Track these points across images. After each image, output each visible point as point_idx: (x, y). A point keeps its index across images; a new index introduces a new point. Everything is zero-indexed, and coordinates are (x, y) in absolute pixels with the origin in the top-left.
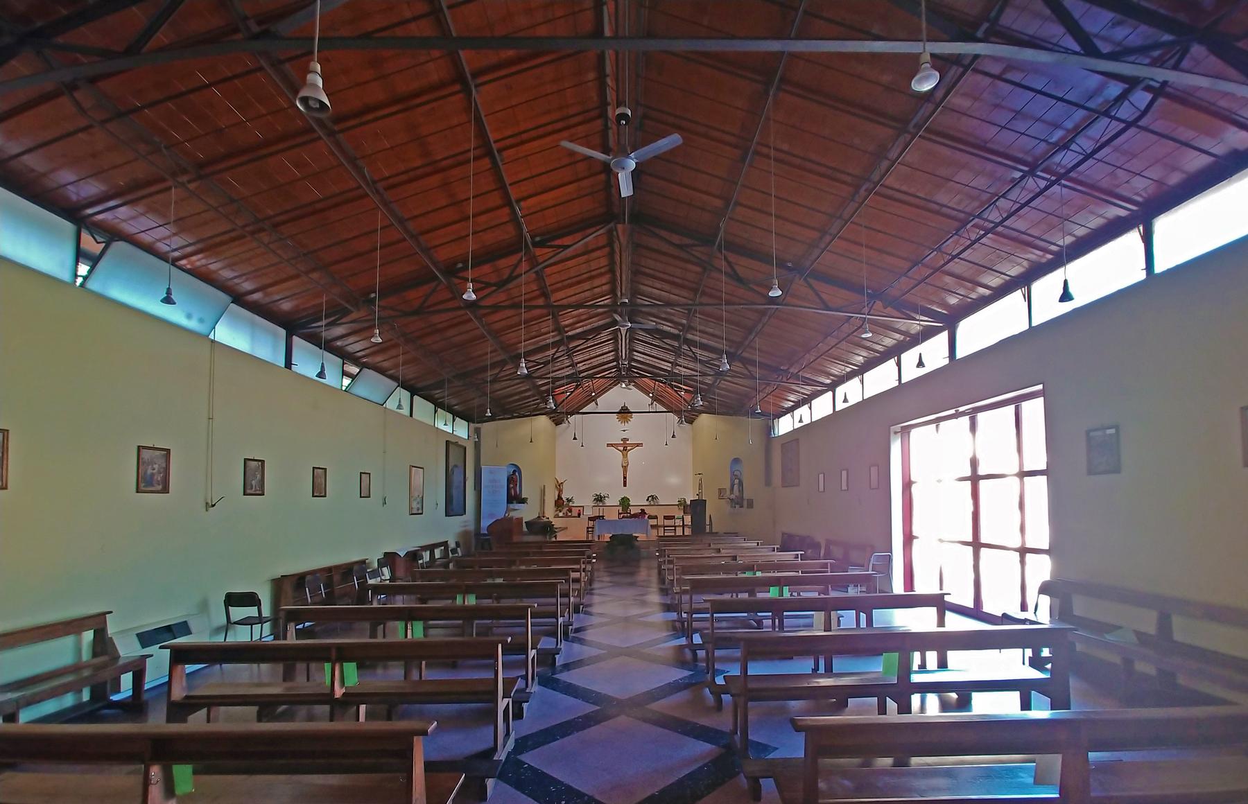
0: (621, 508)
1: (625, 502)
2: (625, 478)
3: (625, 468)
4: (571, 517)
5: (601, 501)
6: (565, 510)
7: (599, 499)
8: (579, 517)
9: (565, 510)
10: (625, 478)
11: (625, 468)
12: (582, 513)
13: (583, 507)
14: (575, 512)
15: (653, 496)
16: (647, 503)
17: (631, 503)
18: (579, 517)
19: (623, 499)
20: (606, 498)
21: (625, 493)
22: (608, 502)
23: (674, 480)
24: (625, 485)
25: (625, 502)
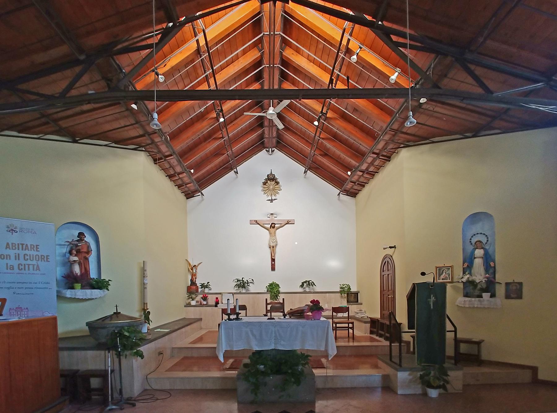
0: (268, 296)
1: (273, 289)
2: (273, 260)
3: (273, 248)
4: (207, 305)
5: (244, 287)
6: (199, 298)
7: (242, 284)
8: (216, 306)
9: (199, 298)
10: (273, 260)
11: (273, 248)
12: (220, 302)
13: (220, 294)
14: (211, 300)
15: (309, 281)
16: (301, 290)
17: (281, 290)
18: (216, 306)
19: (271, 285)
20: (251, 284)
21: (273, 278)
22: (252, 288)
23: (334, 263)
24: (273, 269)
25: (273, 289)
